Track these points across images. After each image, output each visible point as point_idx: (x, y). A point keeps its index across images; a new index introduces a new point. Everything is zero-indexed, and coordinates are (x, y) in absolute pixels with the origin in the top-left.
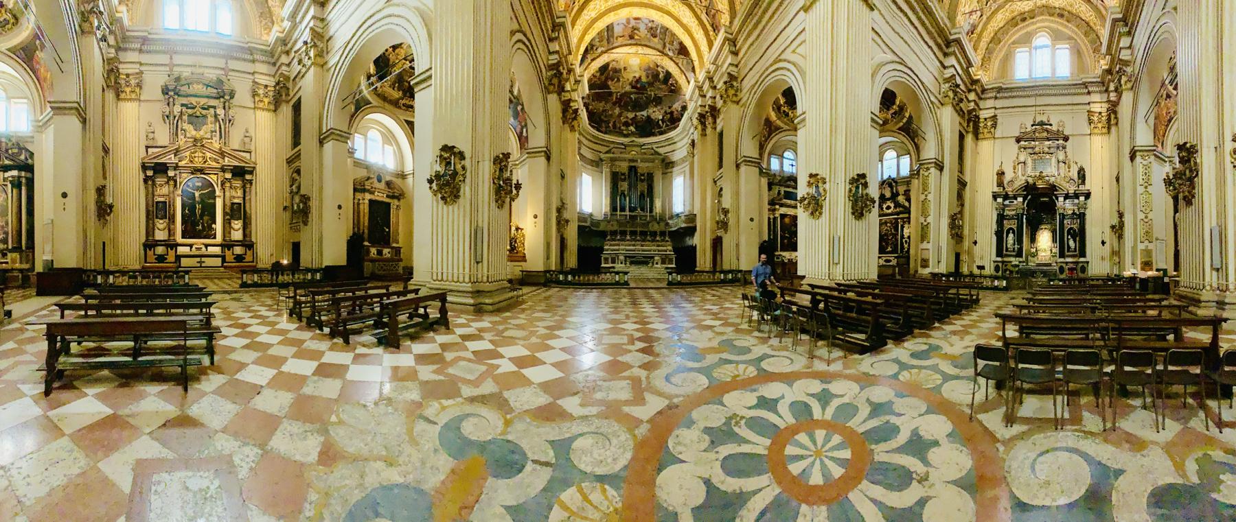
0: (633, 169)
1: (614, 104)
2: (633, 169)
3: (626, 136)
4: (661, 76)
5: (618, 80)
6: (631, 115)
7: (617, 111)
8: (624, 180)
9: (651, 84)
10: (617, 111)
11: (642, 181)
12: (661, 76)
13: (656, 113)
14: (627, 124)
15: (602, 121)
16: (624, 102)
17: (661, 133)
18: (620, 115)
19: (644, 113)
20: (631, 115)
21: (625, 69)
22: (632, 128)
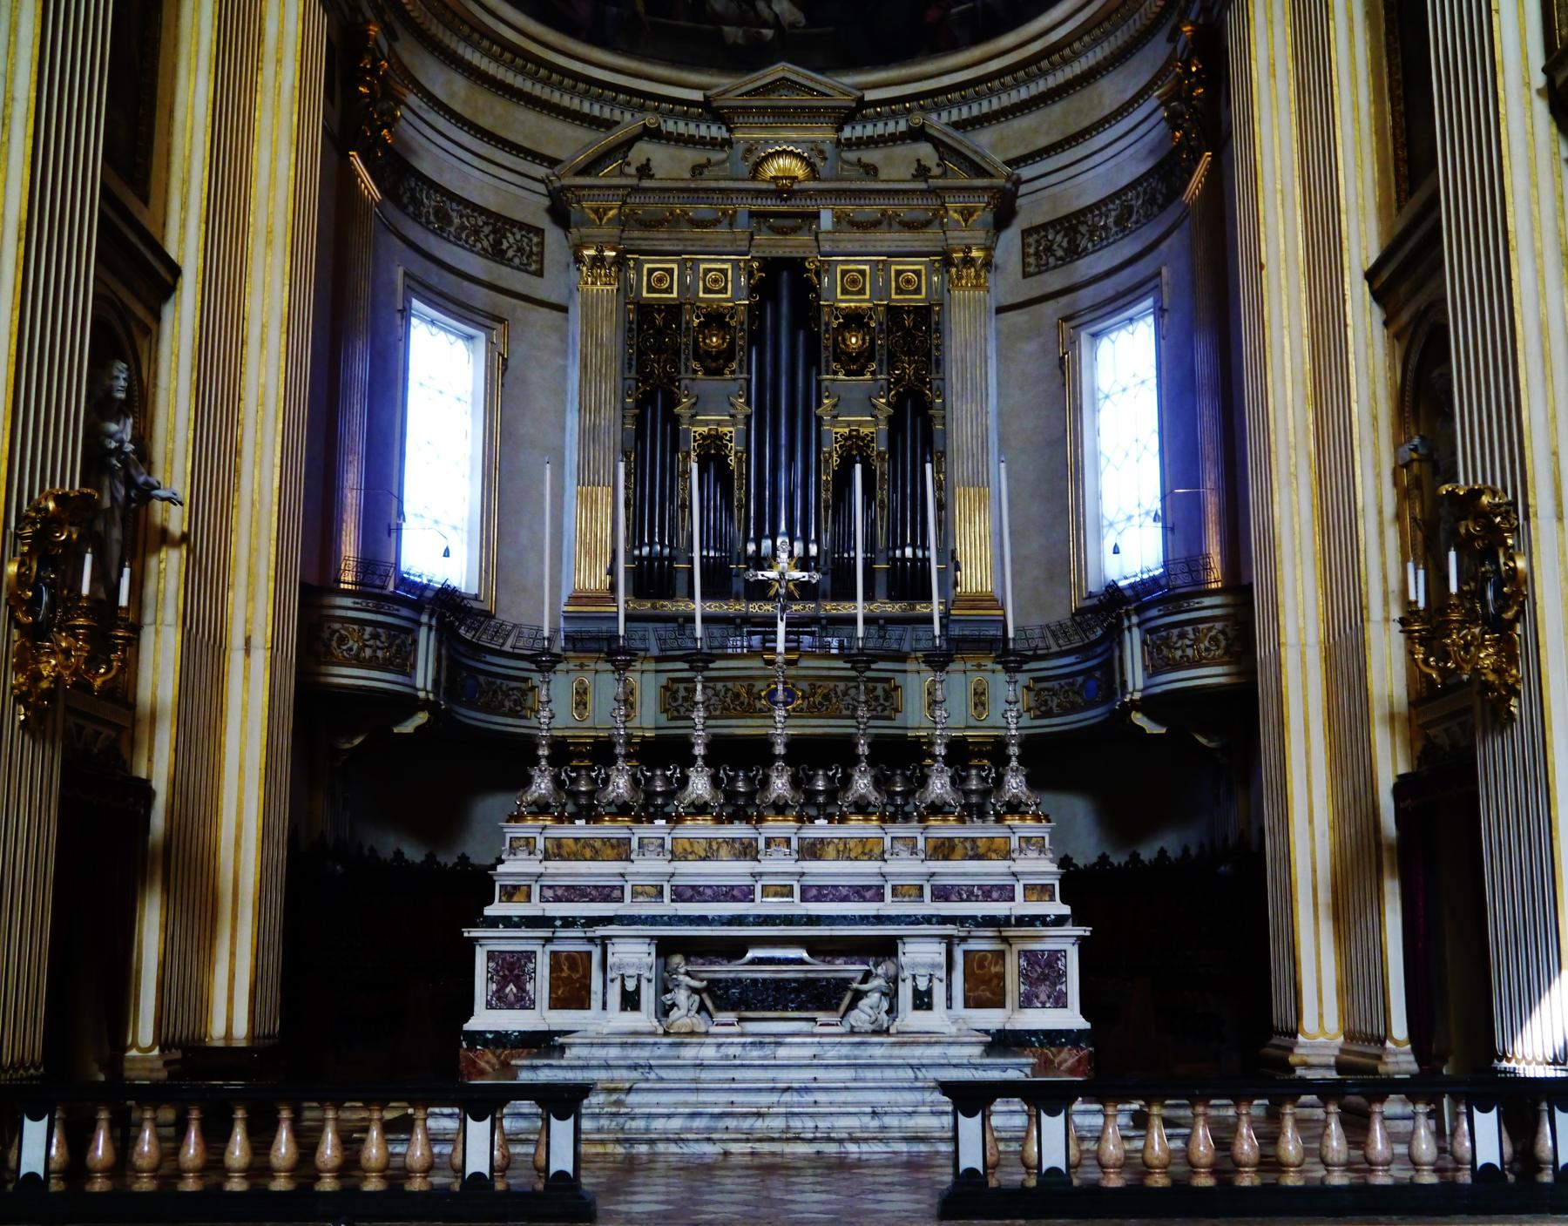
0: (785, 286)
2: (785, 286)
8: (715, 364)
11: (855, 363)
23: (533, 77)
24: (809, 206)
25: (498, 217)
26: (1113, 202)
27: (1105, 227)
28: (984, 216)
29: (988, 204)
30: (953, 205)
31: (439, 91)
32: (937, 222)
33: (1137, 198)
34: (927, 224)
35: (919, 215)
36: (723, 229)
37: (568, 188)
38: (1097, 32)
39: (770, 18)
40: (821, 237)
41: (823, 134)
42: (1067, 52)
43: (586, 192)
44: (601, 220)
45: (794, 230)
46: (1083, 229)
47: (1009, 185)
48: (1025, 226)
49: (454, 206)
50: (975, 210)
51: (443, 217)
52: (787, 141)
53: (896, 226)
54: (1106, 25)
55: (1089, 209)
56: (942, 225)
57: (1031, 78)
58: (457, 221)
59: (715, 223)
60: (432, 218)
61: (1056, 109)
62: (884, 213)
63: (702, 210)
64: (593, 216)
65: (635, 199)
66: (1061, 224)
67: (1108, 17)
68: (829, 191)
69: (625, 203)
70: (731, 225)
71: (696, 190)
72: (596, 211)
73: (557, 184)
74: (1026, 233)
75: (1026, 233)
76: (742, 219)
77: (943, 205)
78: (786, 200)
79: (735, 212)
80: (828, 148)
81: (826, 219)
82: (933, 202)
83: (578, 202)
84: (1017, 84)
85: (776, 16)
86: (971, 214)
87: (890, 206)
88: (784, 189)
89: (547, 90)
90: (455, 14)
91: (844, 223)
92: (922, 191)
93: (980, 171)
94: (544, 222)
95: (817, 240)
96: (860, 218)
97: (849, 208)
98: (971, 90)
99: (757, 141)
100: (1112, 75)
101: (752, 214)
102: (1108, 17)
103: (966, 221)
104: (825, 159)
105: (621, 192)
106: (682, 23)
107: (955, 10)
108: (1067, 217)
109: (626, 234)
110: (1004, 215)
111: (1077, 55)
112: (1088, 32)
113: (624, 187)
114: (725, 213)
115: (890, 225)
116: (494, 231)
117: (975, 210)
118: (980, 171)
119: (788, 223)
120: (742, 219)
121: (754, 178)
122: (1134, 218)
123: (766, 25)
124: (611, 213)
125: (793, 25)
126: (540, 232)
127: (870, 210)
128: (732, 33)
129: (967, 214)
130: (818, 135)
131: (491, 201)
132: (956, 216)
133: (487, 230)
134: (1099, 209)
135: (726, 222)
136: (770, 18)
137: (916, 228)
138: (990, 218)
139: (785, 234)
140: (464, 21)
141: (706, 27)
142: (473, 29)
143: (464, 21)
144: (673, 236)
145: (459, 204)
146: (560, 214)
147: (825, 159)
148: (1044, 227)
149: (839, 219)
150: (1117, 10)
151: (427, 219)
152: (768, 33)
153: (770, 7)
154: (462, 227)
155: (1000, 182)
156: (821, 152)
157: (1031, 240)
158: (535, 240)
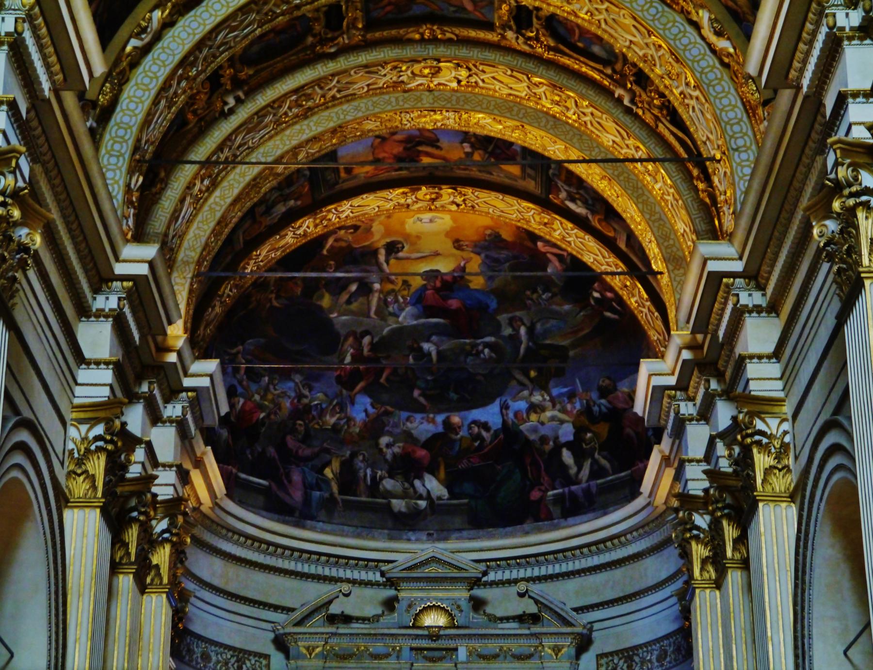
1: (348, 381)
3: (404, 524)
4: (553, 268)
5: (365, 289)
6: (423, 427)
7: (361, 409)
9: (509, 298)
10: (361, 409)
12: (553, 268)
13: (548, 416)
14: (407, 468)
15: (289, 458)
16: (390, 372)
17: (575, 507)
18: (374, 428)
19: (490, 414)
20: (423, 427)
21: (392, 248)
22: (433, 485)
23: (265, 552)
24: (451, 644)
25: (241, 650)
26: (655, 644)
27: (650, 661)
28: (568, 650)
29: (572, 643)
30: (548, 642)
31: (205, 576)
32: (536, 656)
33: (670, 645)
34: (530, 656)
35: (526, 651)
36: (392, 661)
37: (289, 634)
38: (641, 531)
39: (425, 494)
40: (459, 666)
41: (461, 594)
42: (623, 539)
43: (301, 636)
44: (310, 654)
45: (441, 659)
46: (636, 659)
47: (585, 631)
48: (600, 652)
49: (213, 648)
50: (563, 647)
51: (206, 657)
52: (435, 599)
53: (508, 657)
54: (646, 528)
55: (640, 646)
56: (541, 657)
57: (599, 552)
58: (214, 658)
59: (387, 656)
60: (199, 660)
61: (617, 573)
62: (501, 649)
63: (378, 647)
64: (304, 651)
65: (333, 641)
66: (623, 654)
67: (648, 524)
68: (465, 635)
69: (326, 643)
70: (398, 658)
71: (375, 635)
72: (308, 649)
73: (282, 631)
74: (600, 656)
75: (600, 656)
76: (406, 653)
77: (541, 643)
78: (435, 641)
79: (401, 648)
80: (464, 604)
81: (462, 653)
82: (534, 642)
83: (295, 642)
84: (592, 554)
85: (428, 492)
86: (560, 651)
87: (506, 644)
88: (434, 634)
89: (274, 559)
90: (218, 525)
91: (474, 656)
92: (526, 635)
93: (566, 622)
94: (271, 650)
95: (456, 666)
96: (485, 652)
97: (478, 645)
98: (561, 554)
99: (416, 599)
100: (653, 557)
101: (412, 649)
102: (648, 524)
103: (557, 655)
104: (461, 611)
105: (324, 636)
106: (364, 499)
107: (550, 493)
108: (626, 650)
109: (327, 665)
110: (583, 644)
111: (629, 542)
112: (637, 530)
113: (327, 633)
114: (394, 649)
115: (505, 657)
116: (237, 661)
117: (563, 647)
118: (566, 622)
119: (437, 654)
120: (406, 653)
121: (414, 627)
122: (668, 659)
123: (420, 497)
124: (318, 650)
125: (439, 498)
126: (267, 657)
127: (492, 646)
128: (398, 505)
129: (557, 649)
130: (456, 594)
131: (236, 642)
132: (550, 651)
133: (233, 660)
134: (646, 647)
135: (394, 655)
136: (425, 494)
137: (523, 659)
138: (573, 651)
139: (434, 662)
140: (223, 527)
141: (380, 500)
142: (229, 530)
143: (223, 527)
144: (359, 665)
145: (216, 646)
146: (281, 643)
147: (461, 611)
148: (611, 654)
149: (470, 654)
150: (653, 521)
151: (197, 661)
152: (423, 504)
153: (424, 485)
154: (218, 662)
155: (579, 630)
156: (459, 607)
157: (603, 661)
158: (264, 662)
